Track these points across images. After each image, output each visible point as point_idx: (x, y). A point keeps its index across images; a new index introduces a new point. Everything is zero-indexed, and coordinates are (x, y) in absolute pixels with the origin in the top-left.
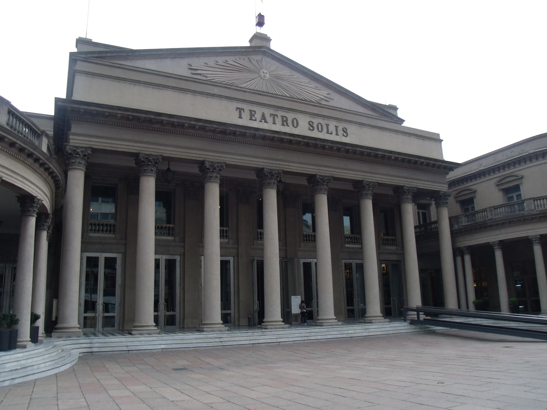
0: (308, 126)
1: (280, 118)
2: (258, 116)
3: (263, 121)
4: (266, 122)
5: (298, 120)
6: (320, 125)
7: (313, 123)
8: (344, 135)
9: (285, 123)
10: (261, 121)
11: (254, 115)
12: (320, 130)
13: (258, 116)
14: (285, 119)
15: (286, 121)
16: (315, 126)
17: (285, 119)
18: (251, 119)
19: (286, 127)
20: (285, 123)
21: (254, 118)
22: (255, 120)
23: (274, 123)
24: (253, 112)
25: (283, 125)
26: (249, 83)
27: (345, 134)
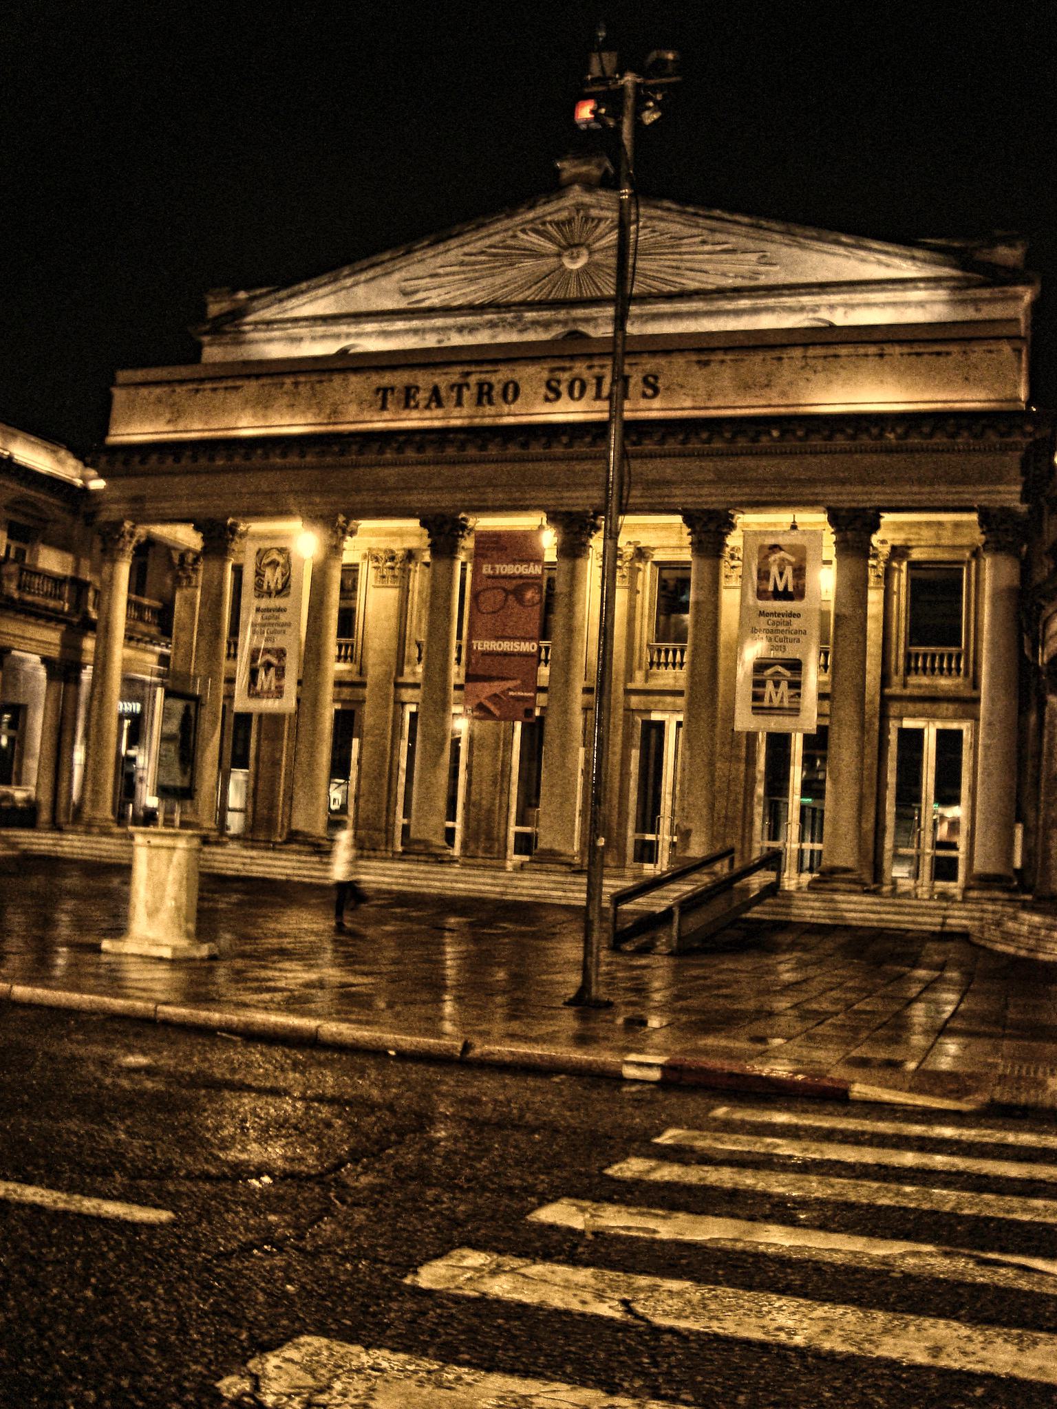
0: (543, 390)
1: (474, 390)
2: (422, 396)
3: (433, 405)
4: (440, 405)
5: (521, 384)
6: (577, 384)
7: (559, 382)
8: (645, 396)
9: (485, 399)
10: (427, 407)
11: (414, 397)
12: (576, 394)
13: (422, 396)
14: (486, 388)
15: (489, 394)
16: (563, 388)
17: (486, 388)
18: (407, 406)
19: (488, 407)
20: (485, 399)
21: (412, 403)
22: (416, 407)
23: (459, 403)
24: (413, 390)
25: (479, 403)
26: (534, 288)
27: (650, 392)
